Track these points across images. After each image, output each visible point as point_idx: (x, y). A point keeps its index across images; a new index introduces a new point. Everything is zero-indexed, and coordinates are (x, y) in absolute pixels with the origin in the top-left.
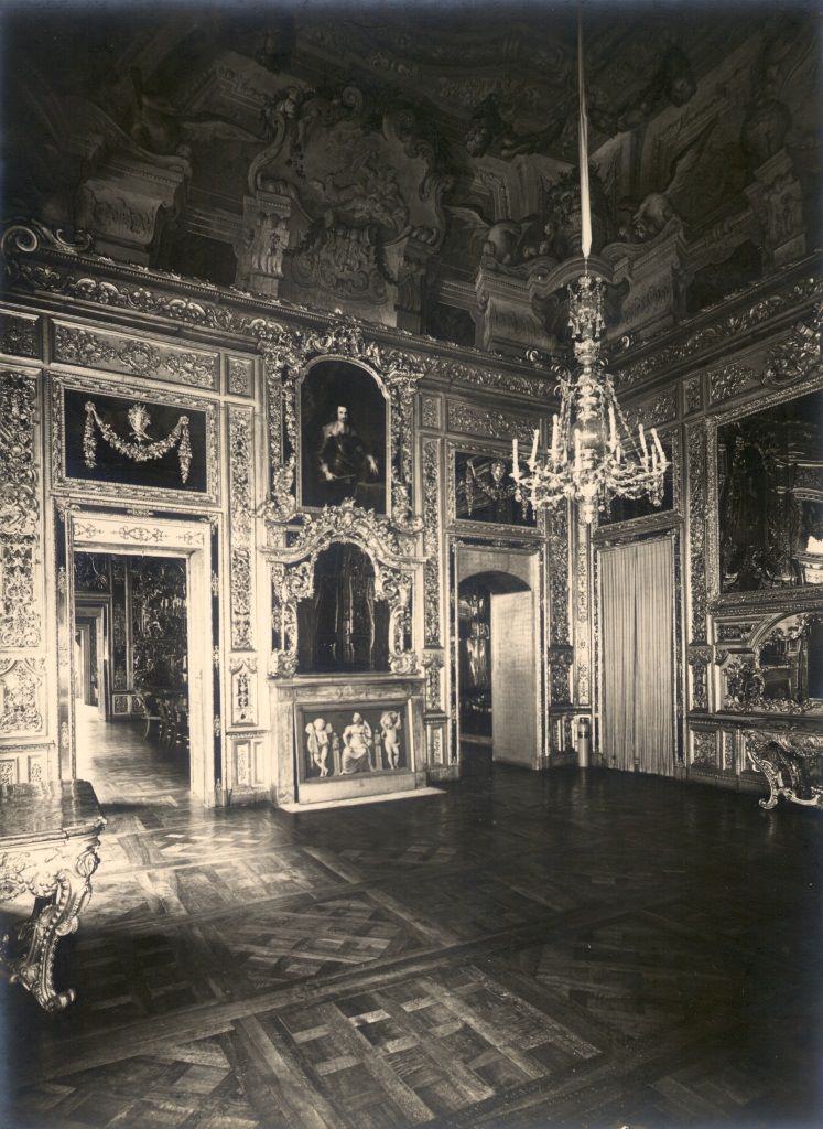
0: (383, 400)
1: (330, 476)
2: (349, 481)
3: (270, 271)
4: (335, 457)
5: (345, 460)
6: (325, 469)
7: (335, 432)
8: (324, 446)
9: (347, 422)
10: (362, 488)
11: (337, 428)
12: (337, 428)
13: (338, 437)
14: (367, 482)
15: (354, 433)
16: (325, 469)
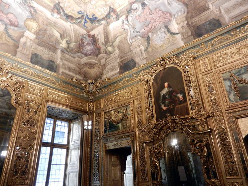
0: (181, 72)
1: (165, 108)
2: (172, 107)
3: (143, 58)
4: (166, 100)
5: (170, 100)
6: (163, 106)
7: (165, 93)
8: (161, 99)
9: (169, 86)
10: (178, 108)
11: (166, 90)
12: (166, 90)
13: (166, 93)
14: (179, 104)
15: (171, 89)
16: (163, 106)
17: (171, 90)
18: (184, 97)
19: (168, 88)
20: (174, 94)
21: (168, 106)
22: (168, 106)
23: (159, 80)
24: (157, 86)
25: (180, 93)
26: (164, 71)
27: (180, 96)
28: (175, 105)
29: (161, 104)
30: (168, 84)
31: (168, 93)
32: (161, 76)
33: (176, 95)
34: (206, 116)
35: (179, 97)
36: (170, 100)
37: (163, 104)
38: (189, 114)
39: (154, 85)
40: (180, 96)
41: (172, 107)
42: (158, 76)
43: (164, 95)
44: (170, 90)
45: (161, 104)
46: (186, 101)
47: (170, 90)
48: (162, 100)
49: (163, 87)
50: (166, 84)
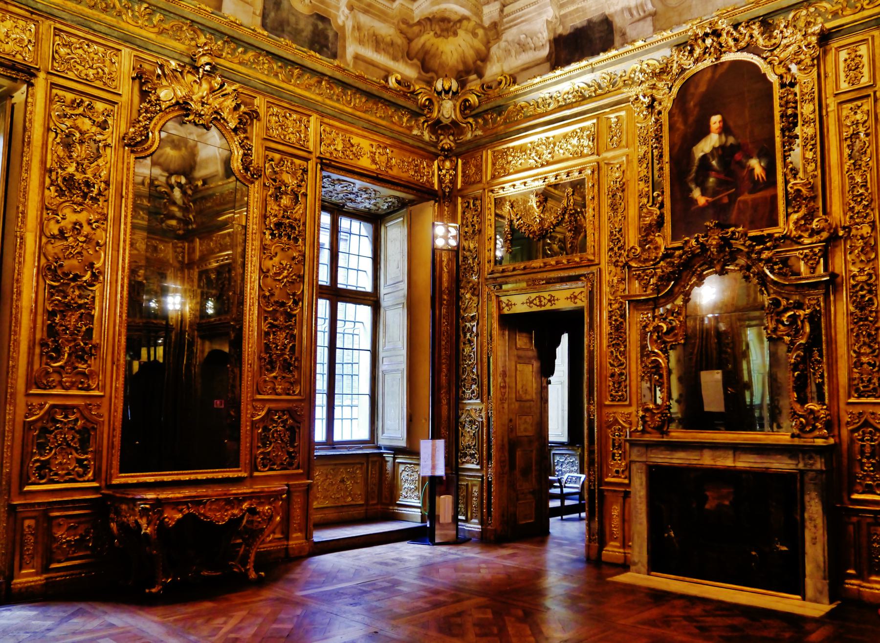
1: (702, 201)
2: (726, 200)
6: (697, 194)
8: (694, 168)
9: (725, 130)
10: (745, 202)
14: (752, 192)
15: (731, 140)
16: (697, 194)
17: (729, 143)
18: (770, 170)
19: (720, 134)
20: (738, 156)
21: (715, 193)
22: (715, 193)
23: (695, 106)
24: (685, 122)
25: (759, 157)
26: (714, 72)
27: (757, 166)
28: (738, 194)
29: (693, 186)
30: (724, 121)
31: (720, 152)
32: (702, 88)
33: (744, 161)
34: (825, 235)
35: (753, 169)
36: (722, 176)
37: (697, 185)
38: (775, 224)
39: (676, 118)
40: (757, 166)
41: (726, 200)
42: (692, 90)
43: (705, 158)
44: (726, 141)
45: (693, 186)
46: (774, 184)
47: (726, 141)
48: (697, 172)
49: (705, 131)
50: (716, 120)
